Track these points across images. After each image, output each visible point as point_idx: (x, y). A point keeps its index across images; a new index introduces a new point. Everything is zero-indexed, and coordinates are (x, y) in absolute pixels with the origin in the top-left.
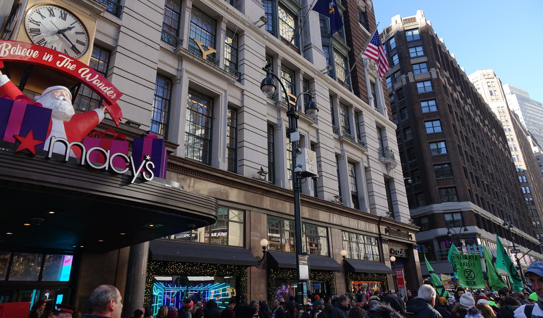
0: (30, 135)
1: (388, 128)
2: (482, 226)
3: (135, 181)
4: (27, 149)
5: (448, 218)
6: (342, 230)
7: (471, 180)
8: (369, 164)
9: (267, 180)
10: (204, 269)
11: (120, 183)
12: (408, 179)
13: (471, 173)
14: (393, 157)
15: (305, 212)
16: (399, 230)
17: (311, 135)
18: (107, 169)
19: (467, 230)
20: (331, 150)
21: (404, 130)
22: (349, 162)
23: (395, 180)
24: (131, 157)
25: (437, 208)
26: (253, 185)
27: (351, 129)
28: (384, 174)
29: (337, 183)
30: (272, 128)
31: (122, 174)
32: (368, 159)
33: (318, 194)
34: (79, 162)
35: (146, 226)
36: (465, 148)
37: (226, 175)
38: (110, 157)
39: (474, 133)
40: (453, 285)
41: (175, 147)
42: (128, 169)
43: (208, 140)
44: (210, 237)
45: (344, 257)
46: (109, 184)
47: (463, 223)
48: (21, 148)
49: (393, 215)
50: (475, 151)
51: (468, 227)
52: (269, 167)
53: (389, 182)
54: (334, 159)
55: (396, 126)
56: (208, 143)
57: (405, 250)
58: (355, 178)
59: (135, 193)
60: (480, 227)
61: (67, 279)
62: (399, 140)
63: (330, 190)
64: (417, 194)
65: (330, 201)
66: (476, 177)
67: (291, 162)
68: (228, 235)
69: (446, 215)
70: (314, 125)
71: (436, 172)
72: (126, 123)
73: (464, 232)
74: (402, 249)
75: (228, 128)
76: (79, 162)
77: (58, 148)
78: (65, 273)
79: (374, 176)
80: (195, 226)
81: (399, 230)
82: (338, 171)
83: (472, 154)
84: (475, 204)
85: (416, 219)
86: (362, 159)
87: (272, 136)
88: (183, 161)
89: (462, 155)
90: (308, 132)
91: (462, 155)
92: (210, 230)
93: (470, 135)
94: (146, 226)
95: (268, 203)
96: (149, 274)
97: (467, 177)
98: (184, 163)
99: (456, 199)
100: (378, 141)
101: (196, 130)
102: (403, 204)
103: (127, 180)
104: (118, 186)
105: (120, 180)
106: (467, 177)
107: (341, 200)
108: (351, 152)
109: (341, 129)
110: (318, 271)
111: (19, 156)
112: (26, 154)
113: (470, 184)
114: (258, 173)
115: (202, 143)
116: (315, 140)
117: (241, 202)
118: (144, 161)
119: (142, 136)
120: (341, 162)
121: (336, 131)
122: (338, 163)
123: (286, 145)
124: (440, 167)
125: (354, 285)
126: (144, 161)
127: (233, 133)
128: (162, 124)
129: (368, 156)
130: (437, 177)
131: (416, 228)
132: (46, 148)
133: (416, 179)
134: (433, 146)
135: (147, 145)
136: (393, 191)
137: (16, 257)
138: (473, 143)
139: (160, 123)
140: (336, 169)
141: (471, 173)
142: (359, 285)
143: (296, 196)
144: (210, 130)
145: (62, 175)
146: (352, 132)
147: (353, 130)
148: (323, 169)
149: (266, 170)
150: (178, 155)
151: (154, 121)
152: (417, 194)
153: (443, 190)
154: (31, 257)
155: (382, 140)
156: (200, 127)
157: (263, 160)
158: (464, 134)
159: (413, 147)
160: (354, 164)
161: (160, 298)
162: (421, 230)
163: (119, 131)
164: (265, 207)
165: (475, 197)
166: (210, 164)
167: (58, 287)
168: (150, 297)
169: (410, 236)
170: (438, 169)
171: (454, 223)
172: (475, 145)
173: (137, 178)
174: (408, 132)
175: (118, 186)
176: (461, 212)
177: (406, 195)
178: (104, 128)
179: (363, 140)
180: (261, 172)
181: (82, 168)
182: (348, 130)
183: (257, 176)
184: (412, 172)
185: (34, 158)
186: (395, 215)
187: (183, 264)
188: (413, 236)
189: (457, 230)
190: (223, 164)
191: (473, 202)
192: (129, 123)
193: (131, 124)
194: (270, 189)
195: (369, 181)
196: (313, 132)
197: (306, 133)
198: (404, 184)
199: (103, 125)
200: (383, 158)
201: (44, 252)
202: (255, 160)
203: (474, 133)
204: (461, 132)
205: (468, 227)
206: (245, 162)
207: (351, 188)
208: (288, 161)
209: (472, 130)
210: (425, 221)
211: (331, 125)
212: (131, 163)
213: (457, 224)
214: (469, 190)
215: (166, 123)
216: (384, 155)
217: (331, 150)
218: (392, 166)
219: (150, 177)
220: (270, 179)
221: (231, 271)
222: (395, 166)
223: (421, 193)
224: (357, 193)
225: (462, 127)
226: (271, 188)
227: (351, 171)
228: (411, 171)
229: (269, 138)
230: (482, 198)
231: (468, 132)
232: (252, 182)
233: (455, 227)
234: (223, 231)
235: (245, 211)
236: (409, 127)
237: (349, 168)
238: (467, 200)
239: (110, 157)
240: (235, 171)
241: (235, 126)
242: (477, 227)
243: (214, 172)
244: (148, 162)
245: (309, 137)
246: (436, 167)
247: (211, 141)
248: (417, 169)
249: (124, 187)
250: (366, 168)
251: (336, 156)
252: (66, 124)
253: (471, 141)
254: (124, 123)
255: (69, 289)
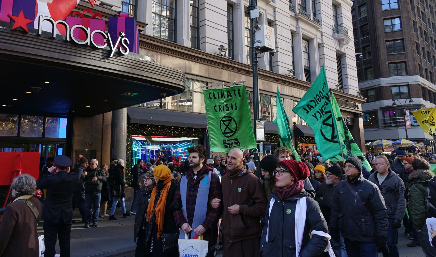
0: (21, 14)
1: (343, 5)
2: (428, 98)
3: (113, 55)
4: (21, 27)
5: (395, 90)
6: (294, 101)
7: (422, 54)
8: (322, 40)
9: (227, 55)
10: (174, 131)
11: (100, 57)
12: (360, 55)
13: (423, 48)
14: (346, 34)
15: (261, 84)
16: (347, 101)
17: (268, 14)
18: (89, 44)
19: (412, 101)
20: (287, 27)
21: (359, 7)
22: (303, 39)
23: (347, 55)
24: (109, 34)
25: (385, 81)
26: (214, 60)
27: (307, 7)
28: (336, 50)
29: (291, 58)
30: (231, 7)
31: (102, 49)
32: (322, 35)
33: (273, 68)
34: (64, 39)
35: (125, 94)
36: (420, 23)
37: (190, 51)
38: (91, 34)
39: (431, 9)
40: (393, 149)
41: (144, 26)
42: (106, 44)
43: (173, 20)
44: (178, 106)
45: (294, 123)
46: (91, 58)
47: (409, 96)
48: (15, 26)
49: (342, 88)
50: (430, 27)
51: (413, 99)
52: (229, 44)
53: (340, 57)
54: (290, 36)
55: (352, 3)
56: (173, 23)
57: (351, 118)
58: (308, 54)
59: (112, 65)
60: (425, 99)
61: (64, 137)
62: (353, 17)
63: (284, 65)
64: (366, 69)
65: (284, 74)
66: (428, 52)
67: (249, 39)
68: (193, 103)
69: (392, 88)
70: (272, 3)
71: (388, 47)
72: (100, 4)
73: (410, 104)
74: (348, 118)
75: (191, 8)
76: (64, 39)
77: (46, 27)
78: (62, 133)
79: (326, 51)
80: (166, 94)
81: (347, 101)
82: (293, 47)
83: (427, 29)
84: (423, 77)
85: (364, 92)
86: (316, 36)
87: (231, 15)
88: (152, 39)
89: (416, 30)
90: (265, 11)
91: (416, 30)
92: (177, 99)
93: (427, 11)
94: (125, 94)
95: (227, 76)
96: (128, 134)
97: (418, 52)
98: (152, 41)
99: (404, 72)
100: (332, 18)
101: (161, 11)
102: (353, 78)
103: (107, 54)
104: (99, 59)
105: (101, 54)
106: (418, 52)
107: (294, 73)
108: (306, 29)
109: (297, 7)
110: (272, 135)
111: (15, 33)
112: (20, 31)
113: (421, 59)
114: (219, 49)
115: (167, 24)
116: (272, 19)
117: (204, 75)
118: (120, 37)
119: (116, 15)
120: (296, 39)
121: (292, 9)
122: (292, 40)
123: (245, 22)
124: (392, 43)
125: (302, 147)
126: (120, 37)
127: (195, 12)
128: (131, 5)
129: (322, 33)
130: (388, 53)
131: (363, 99)
132: (36, 27)
133: (367, 55)
134: (388, 23)
135: (121, 24)
136: (344, 66)
137: (22, 119)
138: (429, 19)
139: (129, 4)
140: (290, 45)
141: (423, 48)
142: (306, 147)
143: (253, 70)
144: (174, 10)
145: (52, 50)
146: (307, 10)
147: (309, 8)
148: (279, 45)
149: (226, 46)
150: (147, 34)
151: (124, 2)
152: (366, 69)
153: (392, 65)
154: (33, 119)
155: (337, 17)
156: (165, 7)
157: (224, 38)
158: (421, 9)
159: (367, 24)
160: (308, 40)
161: (139, 153)
162: (367, 101)
163: (94, 11)
164: (224, 80)
165: (424, 72)
166: (175, 41)
167: (58, 143)
168: (130, 153)
169: (357, 106)
170: (389, 45)
171: (400, 95)
172: (431, 20)
173: (115, 53)
174: (363, 9)
175: (99, 59)
176: (408, 86)
177: (356, 69)
178: (81, 10)
179: (318, 17)
180: (222, 48)
181: (68, 44)
182: (304, 8)
183: (218, 52)
184: (364, 48)
185: (27, 35)
186: (344, 87)
187: (156, 126)
188: (360, 106)
189: (402, 102)
190: (186, 41)
191: (422, 76)
192: (102, 4)
193: (104, 6)
194: (229, 64)
195: (322, 57)
196: (270, 10)
197: (264, 12)
198: (355, 59)
199: (80, 7)
200: (337, 34)
201: (44, 115)
202: (215, 37)
203: (431, 9)
204: (417, 7)
205: (413, 99)
206: (207, 40)
207: (304, 63)
208: (246, 38)
209: (430, 6)
210: (372, 93)
211: (288, 3)
212: (108, 39)
213: (402, 96)
214: (419, 65)
215: (134, 4)
216: (338, 32)
217: (287, 27)
218: (345, 42)
219: (126, 52)
220: (229, 55)
221: (197, 133)
222: (348, 42)
223: (371, 67)
224: (309, 67)
225: (419, 2)
226: (230, 63)
227: (305, 47)
228: (363, 47)
229: (228, 17)
230: (431, 72)
231: (425, 8)
232: (213, 58)
233: (401, 98)
234: (188, 101)
235: (207, 83)
236: (365, 4)
237: (303, 44)
238: (416, 75)
239: (91, 34)
240: (198, 48)
241: (197, 6)
242: (422, 99)
243: (180, 48)
244: (123, 38)
245: (266, 15)
246: (388, 43)
247: (175, 20)
248: (369, 46)
249: (105, 60)
250: (319, 44)
251: (292, 33)
252: (49, 5)
253: (427, 17)
254: (98, 4)
255: (67, 143)
